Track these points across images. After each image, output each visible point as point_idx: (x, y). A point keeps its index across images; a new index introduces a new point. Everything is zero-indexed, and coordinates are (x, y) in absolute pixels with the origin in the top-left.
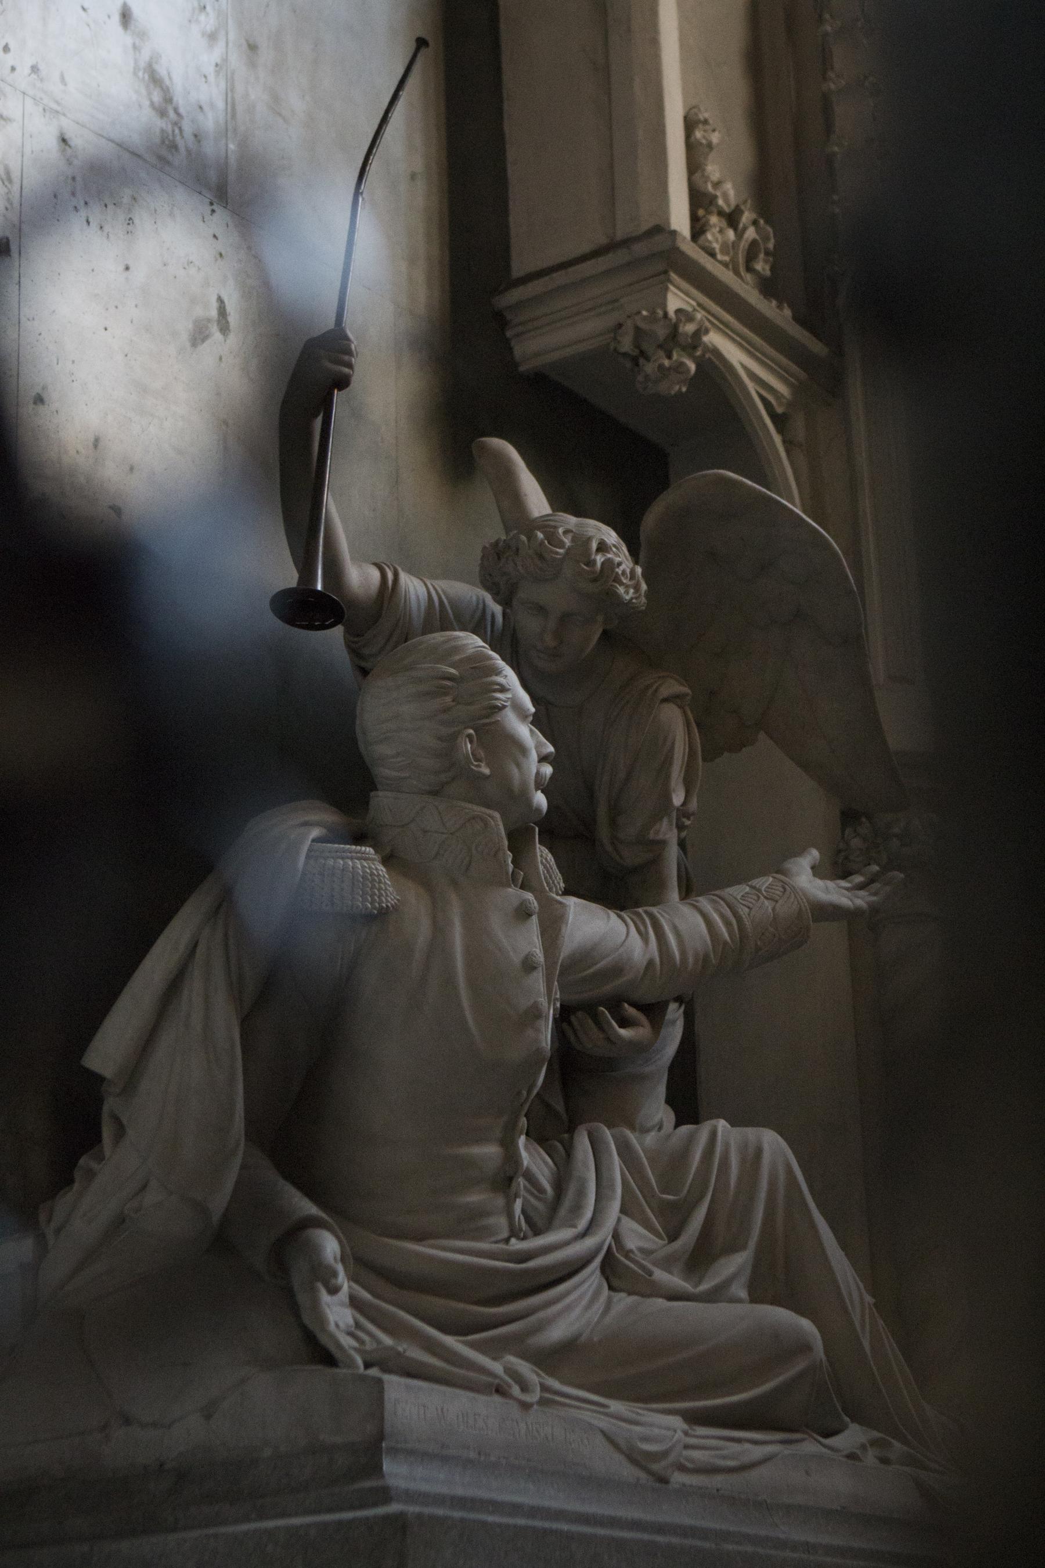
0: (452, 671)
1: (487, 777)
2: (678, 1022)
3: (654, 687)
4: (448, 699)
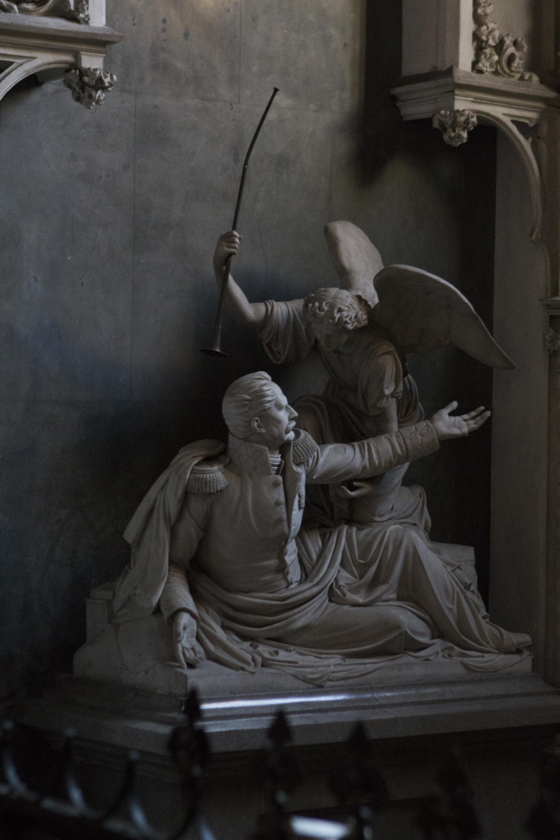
0: (249, 397)
4: (247, 409)
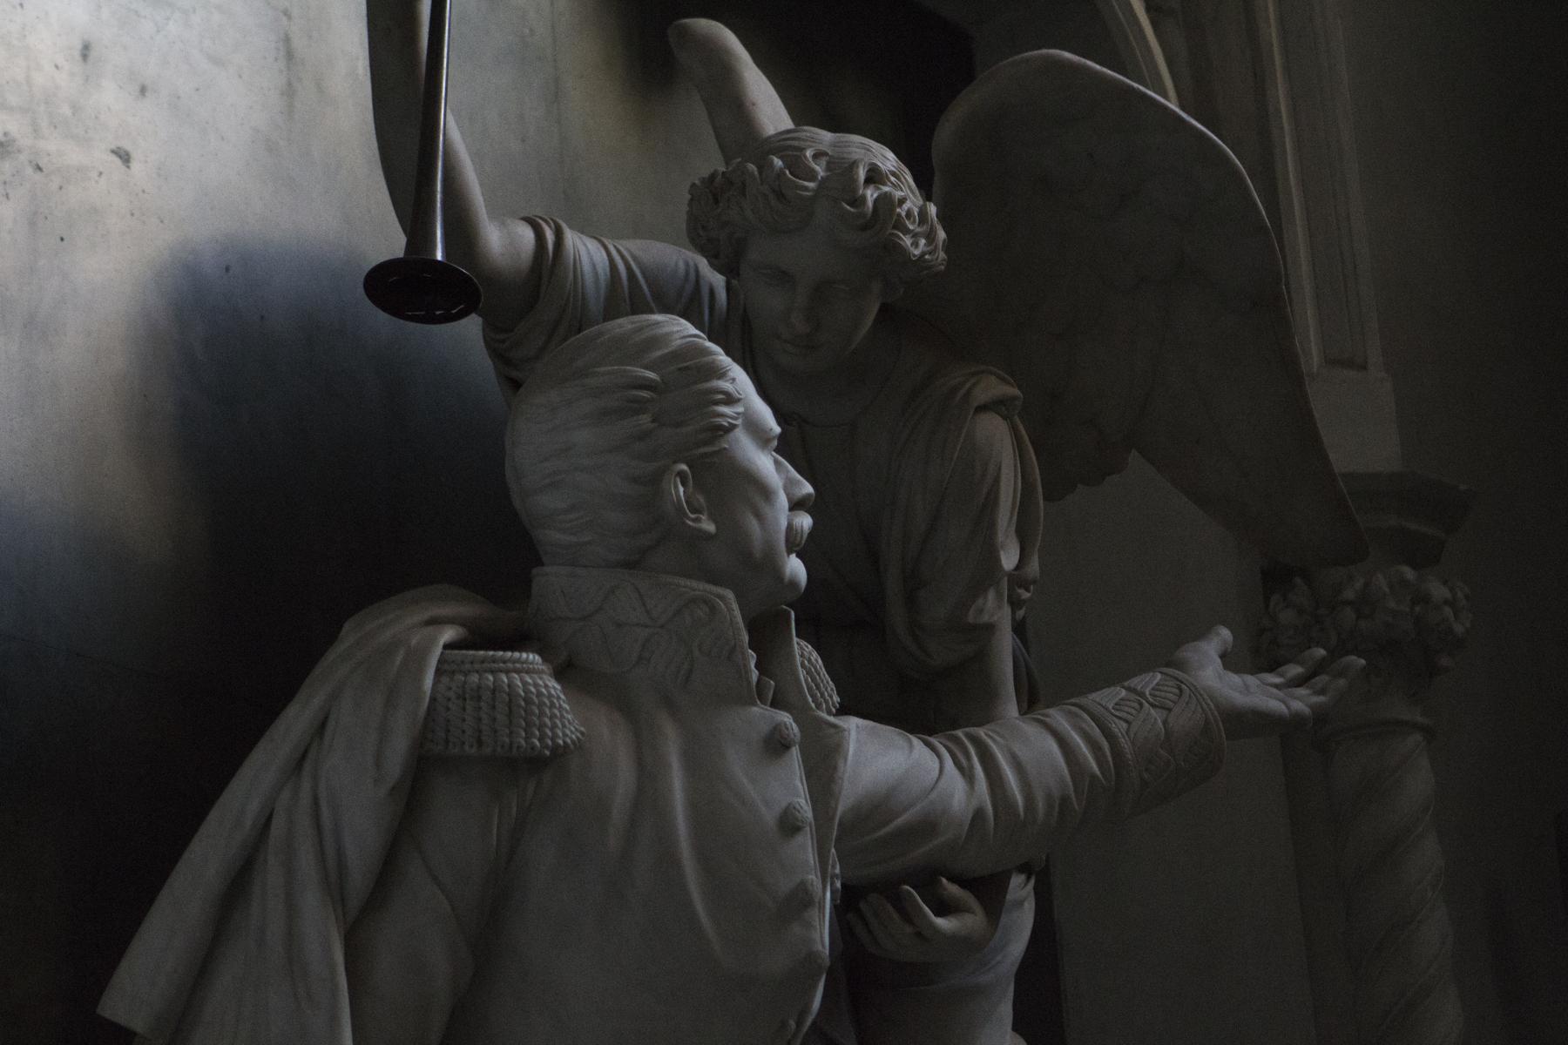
0: (651, 375)
1: (709, 537)
2: (1026, 904)
3: (963, 392)
4: (645, 420)
